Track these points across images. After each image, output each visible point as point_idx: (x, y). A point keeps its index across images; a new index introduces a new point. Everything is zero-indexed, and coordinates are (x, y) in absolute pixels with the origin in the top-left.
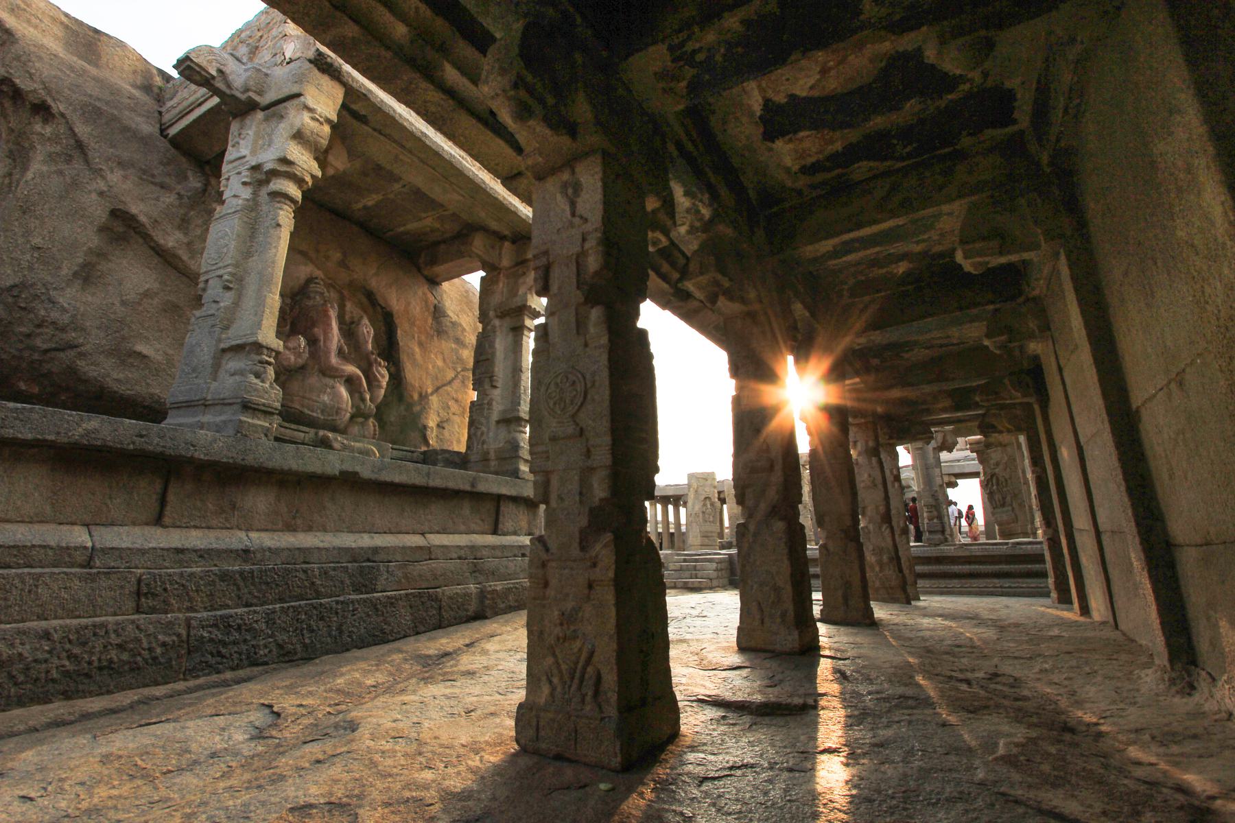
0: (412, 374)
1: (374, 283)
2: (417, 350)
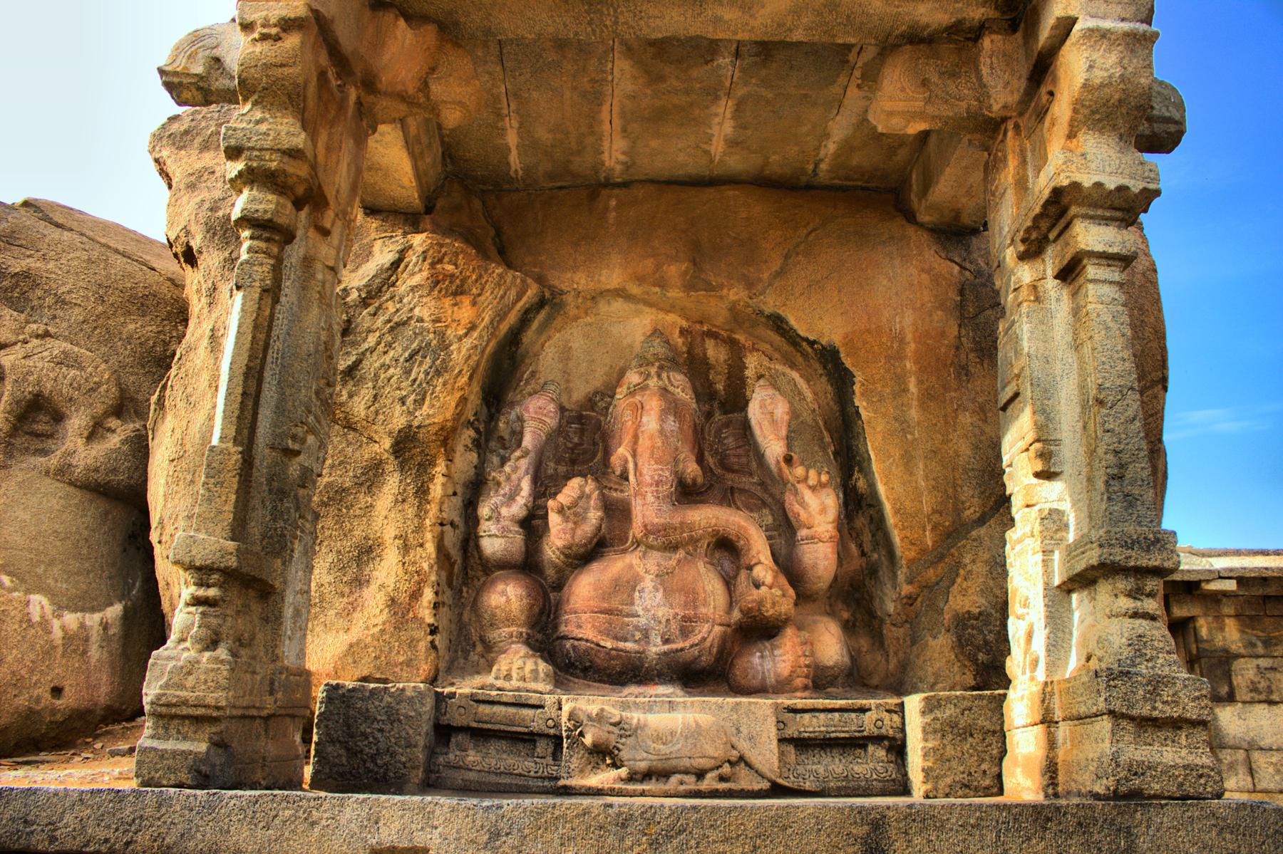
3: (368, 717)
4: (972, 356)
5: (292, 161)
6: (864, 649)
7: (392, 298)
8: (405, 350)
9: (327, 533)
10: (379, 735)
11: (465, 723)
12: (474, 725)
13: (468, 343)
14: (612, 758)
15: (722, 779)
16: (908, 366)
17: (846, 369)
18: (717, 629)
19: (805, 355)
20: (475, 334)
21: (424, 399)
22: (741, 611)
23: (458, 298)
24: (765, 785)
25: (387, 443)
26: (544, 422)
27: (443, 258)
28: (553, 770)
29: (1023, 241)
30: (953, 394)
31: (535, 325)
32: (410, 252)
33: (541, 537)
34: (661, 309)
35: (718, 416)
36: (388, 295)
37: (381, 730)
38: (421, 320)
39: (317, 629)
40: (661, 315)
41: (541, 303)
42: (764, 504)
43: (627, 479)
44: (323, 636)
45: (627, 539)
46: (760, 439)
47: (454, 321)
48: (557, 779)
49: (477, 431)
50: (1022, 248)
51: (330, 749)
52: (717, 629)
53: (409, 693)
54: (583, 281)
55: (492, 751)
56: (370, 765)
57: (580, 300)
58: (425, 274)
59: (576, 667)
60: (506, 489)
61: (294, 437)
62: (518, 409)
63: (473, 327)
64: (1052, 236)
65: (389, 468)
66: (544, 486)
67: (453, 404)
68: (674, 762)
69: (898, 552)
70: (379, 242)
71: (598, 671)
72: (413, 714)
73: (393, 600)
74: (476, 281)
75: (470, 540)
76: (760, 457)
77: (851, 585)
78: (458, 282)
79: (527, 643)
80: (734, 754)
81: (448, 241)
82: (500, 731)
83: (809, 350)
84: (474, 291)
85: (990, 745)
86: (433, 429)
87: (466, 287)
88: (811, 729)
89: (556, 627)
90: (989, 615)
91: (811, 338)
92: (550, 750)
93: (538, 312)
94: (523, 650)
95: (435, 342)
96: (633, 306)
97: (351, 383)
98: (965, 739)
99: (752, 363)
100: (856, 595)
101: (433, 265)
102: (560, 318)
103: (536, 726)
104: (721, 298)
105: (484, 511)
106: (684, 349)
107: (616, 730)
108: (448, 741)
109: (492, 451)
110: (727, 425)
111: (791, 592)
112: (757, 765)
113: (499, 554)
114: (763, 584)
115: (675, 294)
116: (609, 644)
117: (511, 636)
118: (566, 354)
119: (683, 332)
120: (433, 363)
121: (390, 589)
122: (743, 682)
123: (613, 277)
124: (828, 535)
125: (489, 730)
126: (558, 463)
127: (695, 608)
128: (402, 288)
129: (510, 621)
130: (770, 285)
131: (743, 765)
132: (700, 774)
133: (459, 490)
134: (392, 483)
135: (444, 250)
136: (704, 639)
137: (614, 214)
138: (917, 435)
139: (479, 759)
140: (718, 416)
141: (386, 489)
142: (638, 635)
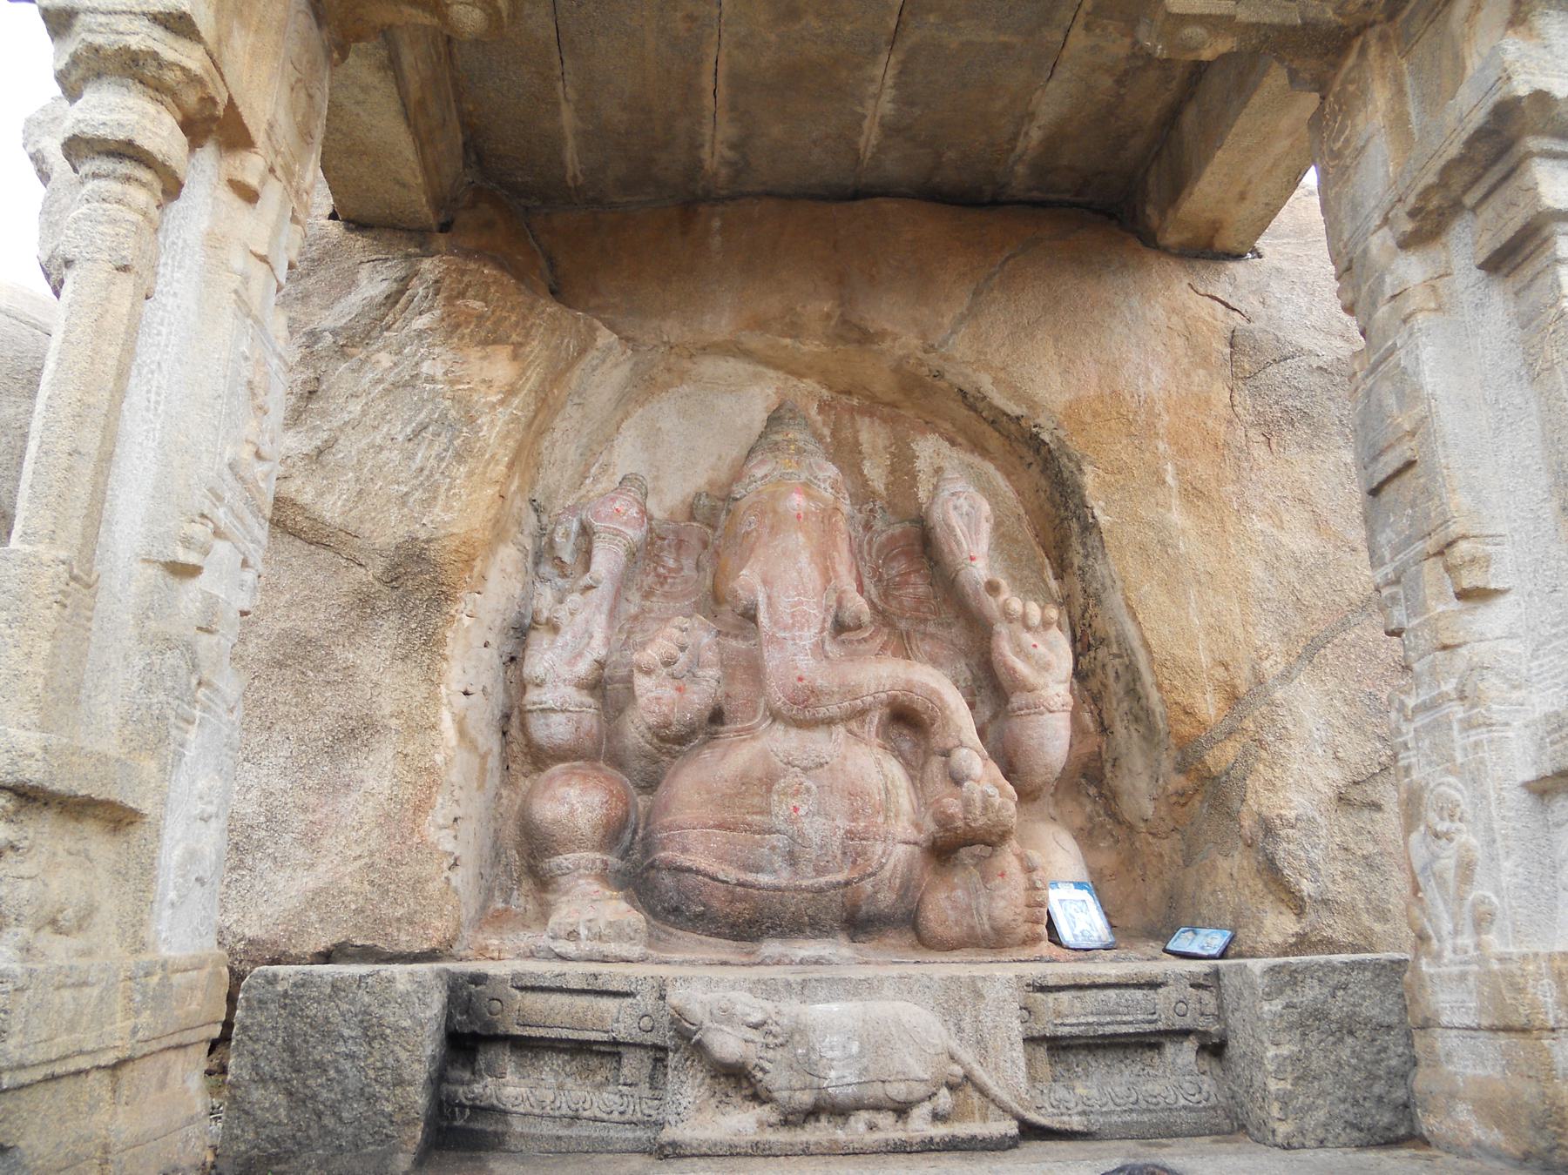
2: (1177, 517)
3: (328, 1034)
5: (169, 38)
8: (405, 424)
9: (282, 709)
10: (347, 1065)
12: (517, 1031)
15: (937, 1117)
16: (1162, 446)
20: (516, 401)
22: (938, 822)
23: (489, 349)
24: (1012, 1128)
25: (378, 566)
28: (648, 1108)
29: (1412, 214)
30: (1230, 488)
32: (415, 281)
33: (621, 711)
36: (380, 343)
37: (351, 1056)
38: (431, 379)
40: (793, 381)
43: (753, 618)
44: (270, 877)
45: (755, 711)
47: (484, 381)
48: (661, 1125)
50: (1408, 226)
51: (257, 1094)
52: (901, 851)
53: (402, 985)
55: (550, 1080)
56: (329, 1121)
58: (437, 313)
60: (566, 636)
61: (187, 542)
64: (1469, 200)
66: (627, 629)
72: (407, 1023)
74: (517, 324)
79: (604, 876)
80: (957, 1070)
81: (472, 266)
82: (561, 1040)
83: (1013, 427)
84: (515, 338)
85: (1385, 1050)
86: (452, 544)
88: (1074, 1021)
90: (1312, 820)
92: (646, 1071)
96: (751, 368)
98: (1341, 1040)
101: (450, 300)
109: (544, 580)
111: (1010, 788)
114: (968, 777)
115: (811, 347)
119: (823, 407)
120: (451, 441)
122: (940, 930)
125: (542, 1038)
132: (902, 1110)
135: (466, 279)
137: (718, 238)
138: (1183, 549)
141: (378, 638)
142: (778, 862)
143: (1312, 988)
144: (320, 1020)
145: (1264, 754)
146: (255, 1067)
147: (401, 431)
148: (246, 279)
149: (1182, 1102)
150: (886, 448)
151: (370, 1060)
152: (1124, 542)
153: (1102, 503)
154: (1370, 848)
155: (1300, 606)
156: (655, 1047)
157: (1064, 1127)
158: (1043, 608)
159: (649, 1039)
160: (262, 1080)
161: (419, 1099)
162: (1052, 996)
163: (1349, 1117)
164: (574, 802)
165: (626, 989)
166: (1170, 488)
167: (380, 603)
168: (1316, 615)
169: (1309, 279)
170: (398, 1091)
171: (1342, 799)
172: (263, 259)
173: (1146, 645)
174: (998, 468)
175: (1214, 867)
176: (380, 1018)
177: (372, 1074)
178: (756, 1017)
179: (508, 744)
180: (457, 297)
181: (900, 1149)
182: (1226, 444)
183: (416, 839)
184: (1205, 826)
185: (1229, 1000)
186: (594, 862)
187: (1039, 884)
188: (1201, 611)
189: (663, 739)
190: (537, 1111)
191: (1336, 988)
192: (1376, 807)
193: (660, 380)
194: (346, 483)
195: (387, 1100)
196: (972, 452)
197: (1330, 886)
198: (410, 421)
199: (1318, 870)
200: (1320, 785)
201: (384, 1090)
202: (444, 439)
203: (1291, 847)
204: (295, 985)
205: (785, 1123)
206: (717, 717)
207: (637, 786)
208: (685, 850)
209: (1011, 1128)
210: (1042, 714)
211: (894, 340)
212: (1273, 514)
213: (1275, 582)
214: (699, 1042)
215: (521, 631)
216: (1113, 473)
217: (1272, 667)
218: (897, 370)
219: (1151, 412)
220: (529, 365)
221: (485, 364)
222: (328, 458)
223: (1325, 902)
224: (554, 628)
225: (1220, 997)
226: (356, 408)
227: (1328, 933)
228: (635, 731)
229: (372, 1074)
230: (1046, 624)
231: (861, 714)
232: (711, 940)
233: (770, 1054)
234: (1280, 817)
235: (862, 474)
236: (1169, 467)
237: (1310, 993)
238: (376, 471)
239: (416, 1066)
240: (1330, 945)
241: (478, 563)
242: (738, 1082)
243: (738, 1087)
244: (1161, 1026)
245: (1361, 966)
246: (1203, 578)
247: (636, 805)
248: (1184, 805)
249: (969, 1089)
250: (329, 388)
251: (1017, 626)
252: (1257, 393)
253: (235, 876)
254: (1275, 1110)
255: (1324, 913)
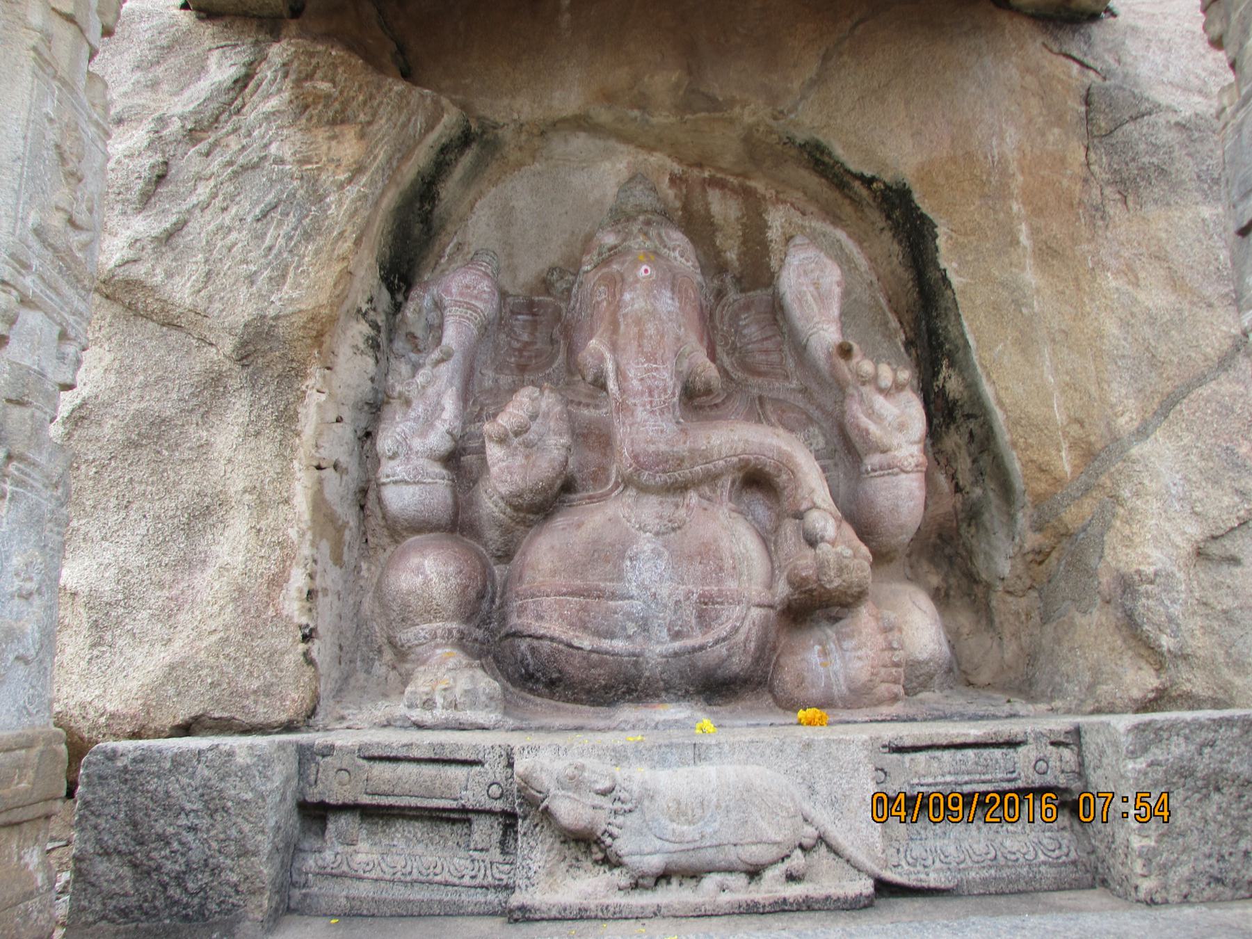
0: (1015, 380)
1: (808, 121)
2: (1031, 277)
3: (169, 807)
4: (1108, 191)
6: (966, 630)
7: (235, 131)
8: (254, 204)
9: (139, 489)
10: (189, 837)
11: (349, 799)
12: (366, 800)
13: (352, 192)
14: (603, 851)
15: (791, 878)
16: (1015, 207)
17: (923, 217)
18: (756, 613)
19: (856, 202)
21: (284, 276)
22: (790, 583)
23: (337, 129)
25: (228, 345)
26: (474, 309)
27: (314, 72)
28: (500, 873)
30: (1085, 247)
31: (458, 172)
32: (264, 65)
33: (475, 482)
34: (641, 146)
35: (732, 295)
36: (229, 127)
37: (193, 829)
39: (120, 642)
41: (465, 139)
42: (811, 420)
43: (604, 387)
44: (128, 652)
45: (608, 480)
46: (800, 324)
47: (331, 161)
48: (509, 888)
49: (375, 326)
51: (102, 866)
52: (756, 613)
53: (241, 759)
54: (526, 109)
55: (400, 843)
56: (175, 892)
57: (523, 137)
58: (286, 95)
59: (538, 680)
60: (419, 409)
62: (434, 290)
63: (359, 170)
65: (234, 383)
66: (477, 401)
67: (330, 282)
68: (709, 855)
69: (1019, 484)
70: (216, 53)
71: (571, 686)
73: (241, 590)
74: (365, 103)
75: (365, 494)
76: (800, 349)
77: (940, 536)
78: (337, 105)
79: (462, 642)
80: (809, 833)
81: (320, 48)
82: (410, 808)
83: (864, 192)
84: (362, 118)
86: (300, 320)
87: (349, 112)
88: (930, 780)
89: (503, 619)
90: (1170, 575)
91: (868, 173)
92: (497, 836)
93: (462, 153)
94: (455, 657)
95: (302, 192)
96: (600, 143)
97: (171, 255)
98: (1207, 796)
99: (777, 220)
100: (948, 551)
101: (298, 83)
102: (494, 165)
103: (472, 798)
104: (731, 122)
105: (385, 443)
106: (678, 204)
107: (605, 802)
108: (323, 830)
109: (399, 357)
110: (747, 307)
111: (864, 550)
112: (850, 850)
113: (411, 512)
114: (822, 539)
115: (662, 119)
116: (586, 643)
117: (435, 637)
118: (506, 218)
119: (674, 180)
120: (300, 221)
121: (236, 572)
123: (568, 98)
124: (913, 461)
125: (391, 807)
126: (499, 369)
127: (720, 581)
128: (251, 116)
129: (431, 612)
130: (803, 97)
131: (823, 849)
132: (754, 873)
133: (347, 414)
134: (239, 409)
135: (314, 61)
136: (736, 630)
137: (567, 16)
138: (1037, 309)
139: (376, 857)
140: (732, 295)
141: (230, 416)
142: (632, 628)
143: (1178, 745)
144: (161, 795)
145: (1121, 511)
146: (99, 841)
147: (247, 207)
148: (48, 38)
149: (1042, 858)
150: (738, 219)
151: (213, 833)
152: (978, 302)
153: (955, 265)
154: (1229, 602)
155: (1155, 363)
156: (504, 813)
157: (919, 884)
158: (895, 371)
159: (498, 805)
160: (107, 854)
161: (266, 871)
162: (907, 757)
163: (1215, 872)
164: (428, 572)
165: (473, 757)
166: (1025, 248)
167: (231, 382)
168: (1171, 371)
169: (1164, 36)
170: (243, 861)
171: (1200, 553)
172: (70, 19)
173: (1000, 403)
174: (850, 236)
175: (1072, 624)
176: (221, 791)
177: (215, 845)
178: (604, 784)
179: (366, 517)
180: (306, 79)
181: (752, 910)
182: (1080, 203)
183: (271, 612)
184: (1062, 584)
185: (1090, 758)
186: (450, 631)
187: (895, 645)
188: (1056, 369)
189: (517, 508)
190: (388, 877)
191: (1203, 745)
192: (1234, 561)
193: (512, 158)
194: (195, 267)
195: (232, 870)
196: (824, 220)
197: (1190, 641)
198: (257, 202)
199: (1178, 625)
200: (1178, 540)
201: (229, 861)
202: (292, 219)
203: (1151, 603)
204: (134, 760)
205: (635, 886)
206: (568, 486)
207: (493, 555)
208: (540, 618)
209: (865, 886)
210: (897, 474)
211: (743, 107)
212: (1129, 272)
213: (1130, 339)
214: (547, 808)
215: (375, 408)
216: (966, 234)
217: (1126, 423)
218: (747, 139)
219: (1004, 173)
220: (376, 146)
221: (334, 143)
222: (180, 241)
223: (1185, 657)
224: (408, 403)
225: (1080, 754)
226: (203, 191)
227: (1187, 687)
228: (491, 501)
229: (215, 845)
230: (898, 387)
231: (712, 478)
232: (569, 706)
233: (620, 820)
234: (1139, 572)
235: (714, 245)
236: (1024, 227)
237: (1178, 749)
238: (225, 251)
239: (260, 837)
240: (1192, 701)
241: (327, 338)
242: (588, 847)
243: (588, 851)
244: (1020, 784)
245: (1229, 722)
246: (1059, 337)
247: (492, 574)
248: (1040, 563)
249: (823, 849)
250: (178, 172)
251: (867, 390)
252: (1112, 150)
253: (95, 653)
254: (1138, 867)
255: (1182, 666)
